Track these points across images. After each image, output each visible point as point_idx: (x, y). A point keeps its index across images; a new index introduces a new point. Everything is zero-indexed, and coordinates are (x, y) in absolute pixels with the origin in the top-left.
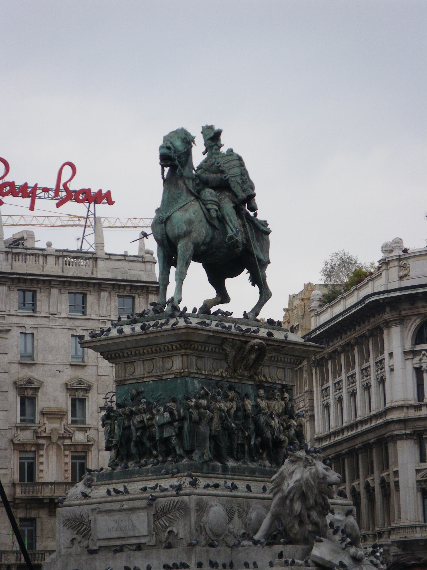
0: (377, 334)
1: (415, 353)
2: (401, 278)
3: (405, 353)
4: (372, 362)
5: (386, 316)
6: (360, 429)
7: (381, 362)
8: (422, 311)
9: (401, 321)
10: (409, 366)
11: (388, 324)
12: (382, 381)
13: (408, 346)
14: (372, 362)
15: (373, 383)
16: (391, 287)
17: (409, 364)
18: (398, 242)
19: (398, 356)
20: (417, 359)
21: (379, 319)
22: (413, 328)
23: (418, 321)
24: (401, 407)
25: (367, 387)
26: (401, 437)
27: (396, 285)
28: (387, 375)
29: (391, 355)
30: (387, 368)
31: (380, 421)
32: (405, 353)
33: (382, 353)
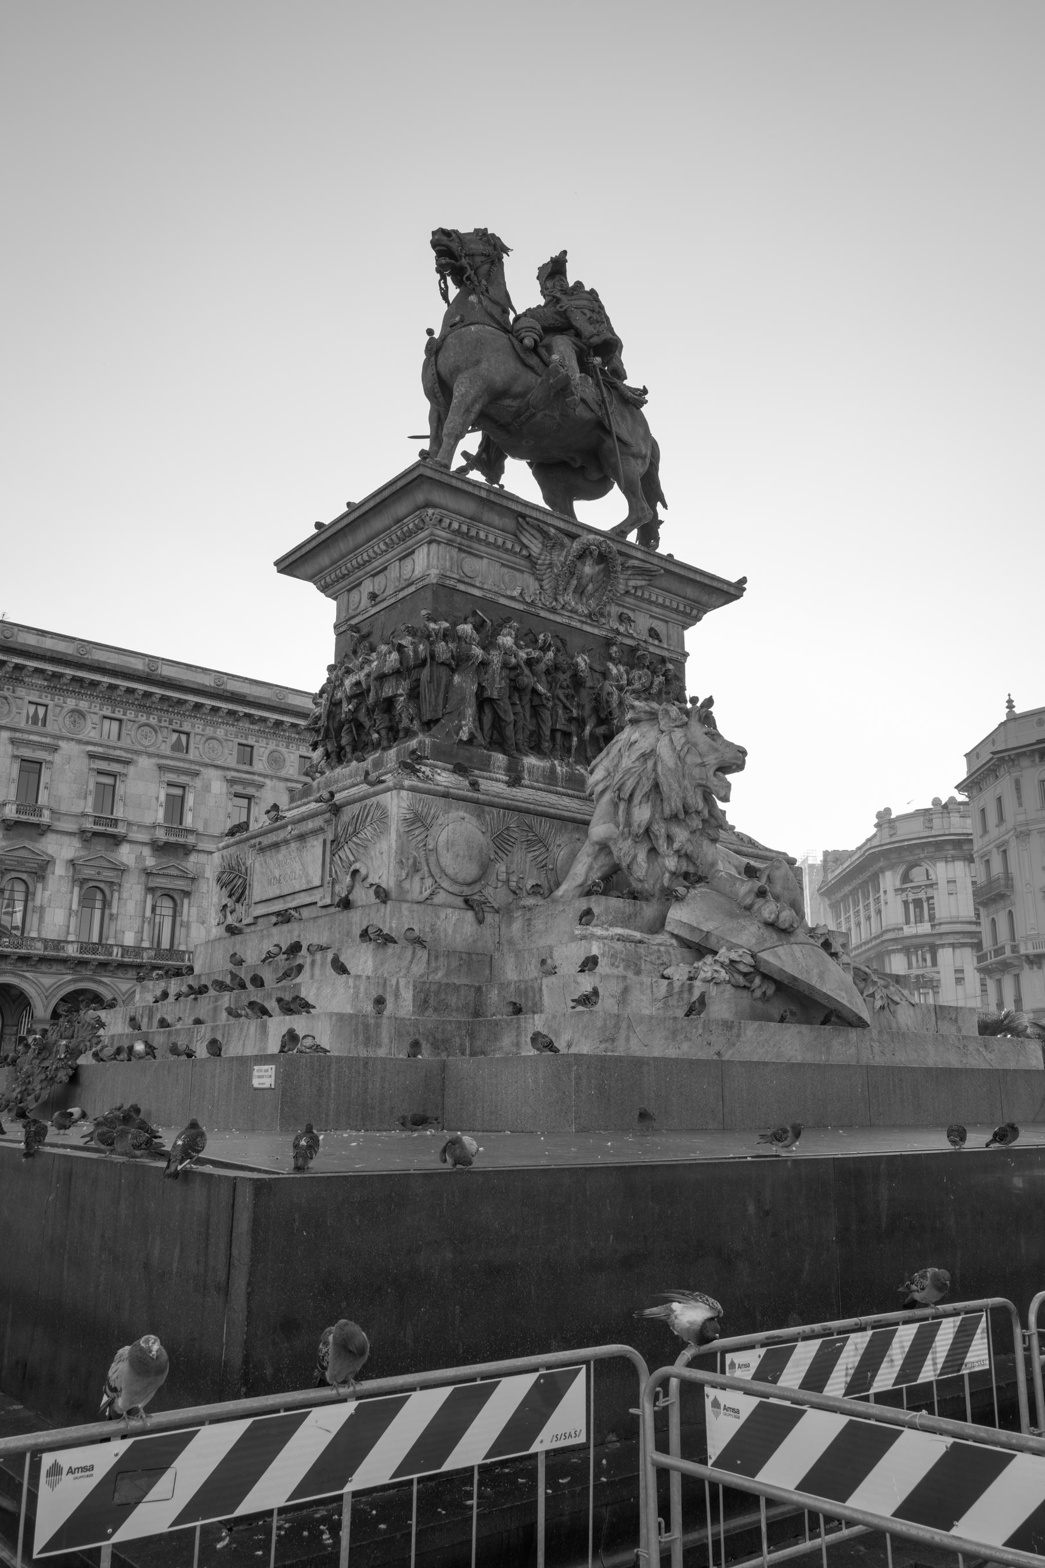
0: (875, 878)
1: (903, 890)
2: (891, 836)
3: (896, 890)
4: (871, 900)
5: (881, 864)
6: (864, 948)
7: (878, 898)
8: (907, 859)
9: (892, 867)
10: (899, 900)
11: (882, 870)
12: (879, 912)
13: (898, 884)
14: (871, 900)
15: (873, 914)
16: (883, 842)
17: (899, 897)
18: (888, 811)
19: (891, 893)
20: (904, 894)
21: (876, 867)
22: (901, 872)
23: (904, 867)
24: (894, 930)
25: (869, 918)
26: (894, 951)
27: (888, 841)
28: (883, 908)
29: (885, 892)
30: (882, 902)
31: (878, 941)
32: (896, 890)
33: (879, 892)
